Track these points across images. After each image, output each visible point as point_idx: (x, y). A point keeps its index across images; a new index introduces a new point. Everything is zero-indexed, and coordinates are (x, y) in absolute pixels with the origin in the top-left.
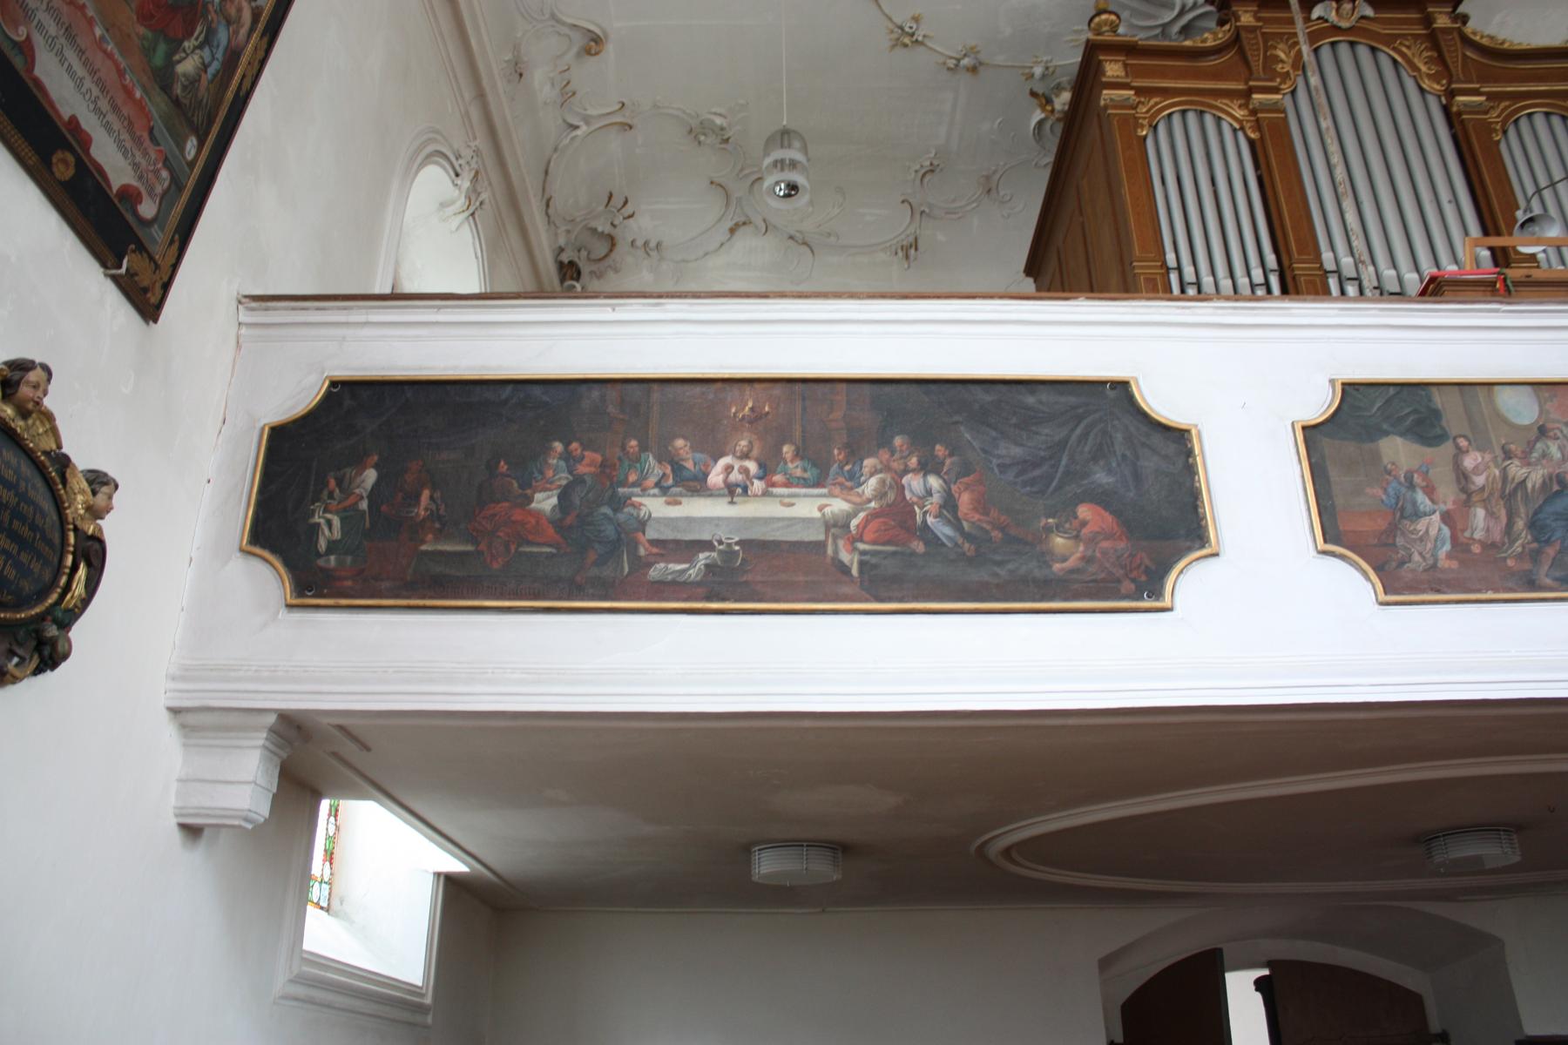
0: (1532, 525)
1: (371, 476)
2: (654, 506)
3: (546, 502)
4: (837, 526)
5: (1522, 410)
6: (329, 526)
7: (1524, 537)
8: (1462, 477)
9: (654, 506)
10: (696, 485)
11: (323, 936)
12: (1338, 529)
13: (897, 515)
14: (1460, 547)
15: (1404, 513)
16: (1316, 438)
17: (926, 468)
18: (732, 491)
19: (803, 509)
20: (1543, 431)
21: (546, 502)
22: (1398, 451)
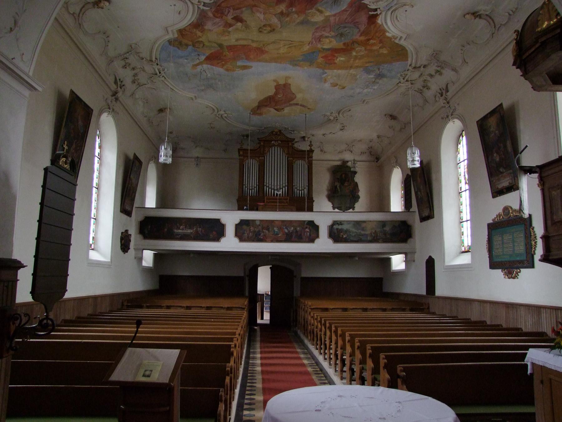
0: (256, 235)
1: (150, 227)
2: (176, 231)
3: (166, 230)
4: (191, 233)
5: (258, 223)
6: (146, 232)
7: (254, 236)
8: (250, 230)
9: (176, 231)
10: (179, 229)
11: (144, 264)
12: (236, 235)
13: (197, 232)
14: (248, 237)
15: (244, 233)
16: (236, 225)
17: (200, 227)
18: (182, 229)
19: (189, 231)
20: (259, 225)
21: (166, 230)
22: (245, 227)
